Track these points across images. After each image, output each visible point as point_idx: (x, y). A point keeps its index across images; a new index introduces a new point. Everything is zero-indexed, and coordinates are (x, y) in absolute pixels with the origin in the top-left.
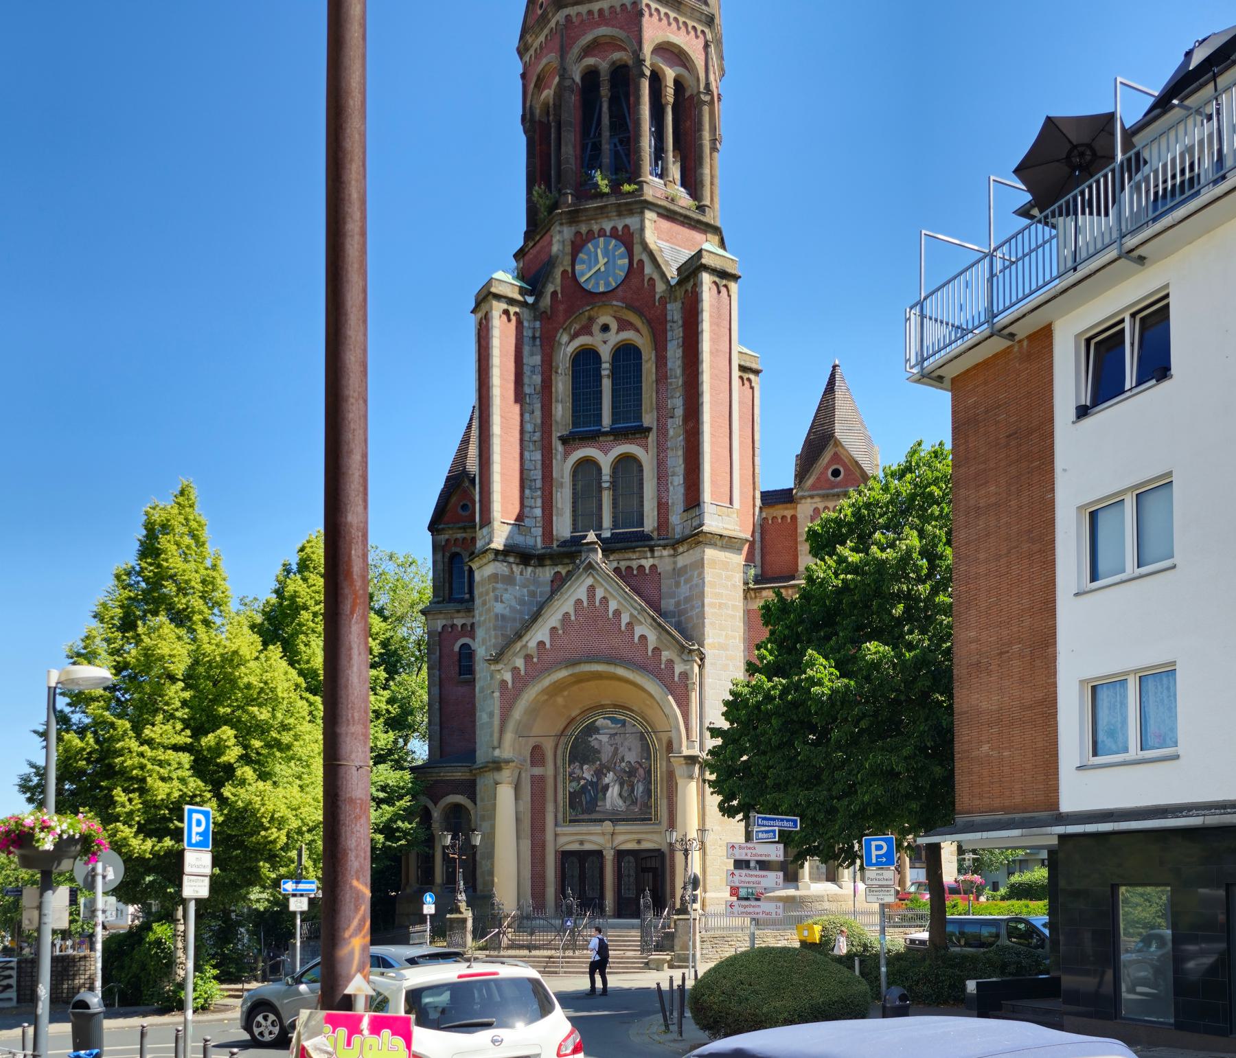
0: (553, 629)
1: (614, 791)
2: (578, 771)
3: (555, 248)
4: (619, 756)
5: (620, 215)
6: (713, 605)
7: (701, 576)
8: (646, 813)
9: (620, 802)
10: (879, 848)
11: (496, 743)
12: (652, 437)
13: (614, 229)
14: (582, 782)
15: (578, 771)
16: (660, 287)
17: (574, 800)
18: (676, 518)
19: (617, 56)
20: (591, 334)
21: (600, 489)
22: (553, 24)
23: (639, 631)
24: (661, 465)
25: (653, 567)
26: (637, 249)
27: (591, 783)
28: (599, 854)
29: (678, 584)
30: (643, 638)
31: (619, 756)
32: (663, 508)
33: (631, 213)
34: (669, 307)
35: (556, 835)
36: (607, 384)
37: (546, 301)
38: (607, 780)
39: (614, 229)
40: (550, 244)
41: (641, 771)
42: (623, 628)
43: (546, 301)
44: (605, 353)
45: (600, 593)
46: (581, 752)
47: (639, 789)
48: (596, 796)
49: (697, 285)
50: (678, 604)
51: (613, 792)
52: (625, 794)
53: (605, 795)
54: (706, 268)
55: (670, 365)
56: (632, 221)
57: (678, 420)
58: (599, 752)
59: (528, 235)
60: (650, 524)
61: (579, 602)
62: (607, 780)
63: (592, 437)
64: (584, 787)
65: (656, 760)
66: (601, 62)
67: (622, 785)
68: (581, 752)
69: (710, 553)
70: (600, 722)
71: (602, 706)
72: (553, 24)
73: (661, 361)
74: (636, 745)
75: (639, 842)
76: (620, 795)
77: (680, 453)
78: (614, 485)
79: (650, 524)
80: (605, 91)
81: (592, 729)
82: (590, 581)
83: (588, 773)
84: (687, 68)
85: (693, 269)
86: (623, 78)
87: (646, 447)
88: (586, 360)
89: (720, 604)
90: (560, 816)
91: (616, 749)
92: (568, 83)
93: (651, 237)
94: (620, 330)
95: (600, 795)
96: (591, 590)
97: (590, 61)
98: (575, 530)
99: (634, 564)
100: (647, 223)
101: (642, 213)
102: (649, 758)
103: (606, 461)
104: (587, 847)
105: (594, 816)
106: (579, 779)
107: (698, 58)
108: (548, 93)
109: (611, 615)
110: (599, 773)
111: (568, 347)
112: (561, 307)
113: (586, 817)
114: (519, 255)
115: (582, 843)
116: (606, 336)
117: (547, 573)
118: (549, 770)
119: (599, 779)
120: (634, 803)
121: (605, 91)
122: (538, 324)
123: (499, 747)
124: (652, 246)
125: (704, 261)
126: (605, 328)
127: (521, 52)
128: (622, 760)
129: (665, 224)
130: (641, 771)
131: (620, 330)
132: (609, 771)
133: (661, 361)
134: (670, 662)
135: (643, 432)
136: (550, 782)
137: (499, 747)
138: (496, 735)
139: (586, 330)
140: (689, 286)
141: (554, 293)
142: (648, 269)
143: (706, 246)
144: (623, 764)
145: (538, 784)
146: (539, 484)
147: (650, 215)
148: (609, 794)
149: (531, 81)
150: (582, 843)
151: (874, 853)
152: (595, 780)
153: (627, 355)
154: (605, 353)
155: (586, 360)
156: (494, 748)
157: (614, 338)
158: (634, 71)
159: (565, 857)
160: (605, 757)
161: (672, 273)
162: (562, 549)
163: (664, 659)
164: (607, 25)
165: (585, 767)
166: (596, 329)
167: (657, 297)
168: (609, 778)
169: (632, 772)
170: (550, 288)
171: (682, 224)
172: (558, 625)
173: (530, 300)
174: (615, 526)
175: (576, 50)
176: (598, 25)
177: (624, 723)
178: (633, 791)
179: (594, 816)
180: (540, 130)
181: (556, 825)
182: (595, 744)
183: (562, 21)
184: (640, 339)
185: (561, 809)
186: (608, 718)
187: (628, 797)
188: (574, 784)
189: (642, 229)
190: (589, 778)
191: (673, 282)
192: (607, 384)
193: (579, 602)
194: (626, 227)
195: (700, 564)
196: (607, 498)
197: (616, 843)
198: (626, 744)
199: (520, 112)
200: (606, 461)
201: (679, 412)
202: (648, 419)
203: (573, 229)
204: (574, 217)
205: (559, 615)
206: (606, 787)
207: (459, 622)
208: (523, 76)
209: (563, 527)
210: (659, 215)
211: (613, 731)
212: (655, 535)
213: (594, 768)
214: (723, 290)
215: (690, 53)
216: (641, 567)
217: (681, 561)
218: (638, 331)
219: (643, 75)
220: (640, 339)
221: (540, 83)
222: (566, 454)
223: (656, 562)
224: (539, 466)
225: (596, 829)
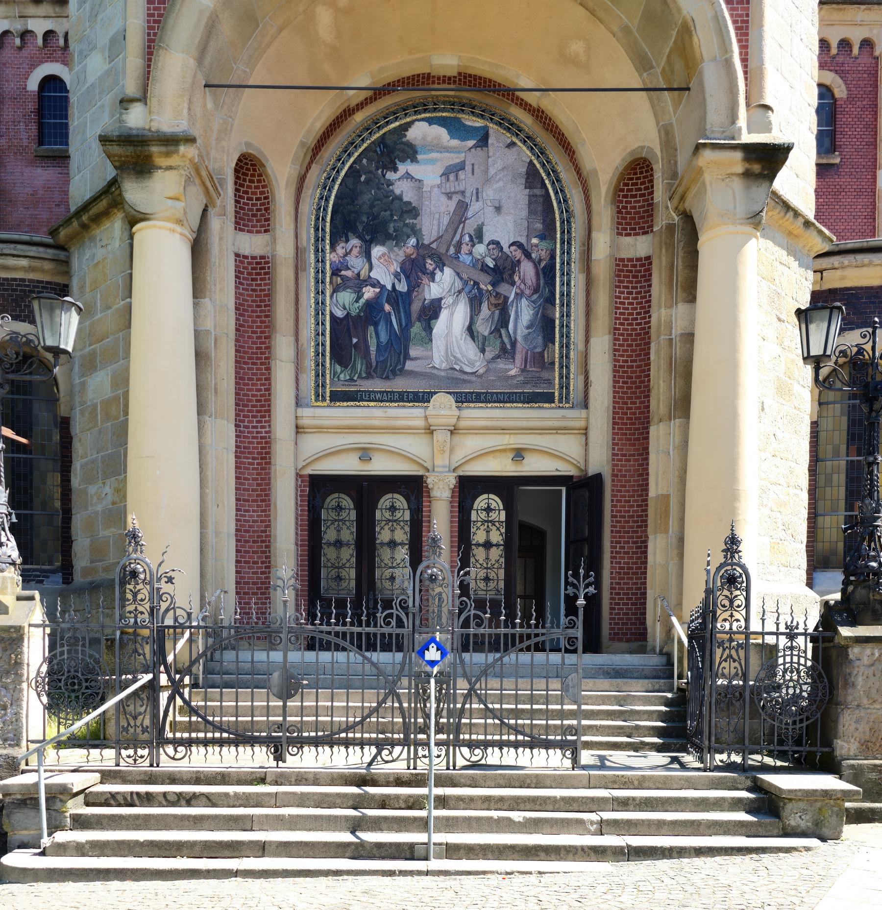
1: (453, 320)
2: (357, 263)
4: (470, 227)
8: (539, 381)
11: (131, 88)
14: (369, 293)
15: (357, 263)
17: (344, 340)
27: (394, 297)
28: (413, 487)
31: (470, 227)
35: (299, 429)
38: (433, 290)
41: (527, 270)
46: (362, 211)
47: (523, 315)
48: (406, 328)
51: (453, 320)
52: (483, 329)
53: (429, 329)
58: (413, 211)
62: (433, 290)
64: (372, 307)
65: (567, 242)
67: (475, 304)
68: (362, 211)
70: (420, 131)
74: (516, 197)
75: (519, 454)
76: (471, 331)
81: (394, 151)
83: (383, 267)
90: (309, 381)
91: (463, 207)
95: (416, 329)
104: (381, 466)
105: (399, 384)
106: (359, 283)
110: (415, 270)
113: (377, 385)
115: (365, 454)
118: (284, 250)
119: (414, 286)
120: (507, 352)
123: (143, 98)
128: (478, 236)
130: (527, 270)
132: (441, 264)
136: (284, 275)
137: (143, 98)
138: (133, 60)
144: (480, 249)
145: (255, 274)
148: (439, 326)
150: (365, 454)
152: (402, 287)
156: (125, 102)
159: (318, 488)
160: (432, 224)
165: (377, 251)
168: (442, 284)
169: (502, 271)
178: (504, 321)
179: (399, 384)
181: (298, 404)
182: (403, 189)
185: (310, 364)
186: (443, 122)
187: (495, 338)
188: (346, 296)
190: (387, 281)
197: (459, 455)
198: (489, 193)
206: (432, 310)
211: (455, 159)
213: (400, 254)
225: (411, 415)
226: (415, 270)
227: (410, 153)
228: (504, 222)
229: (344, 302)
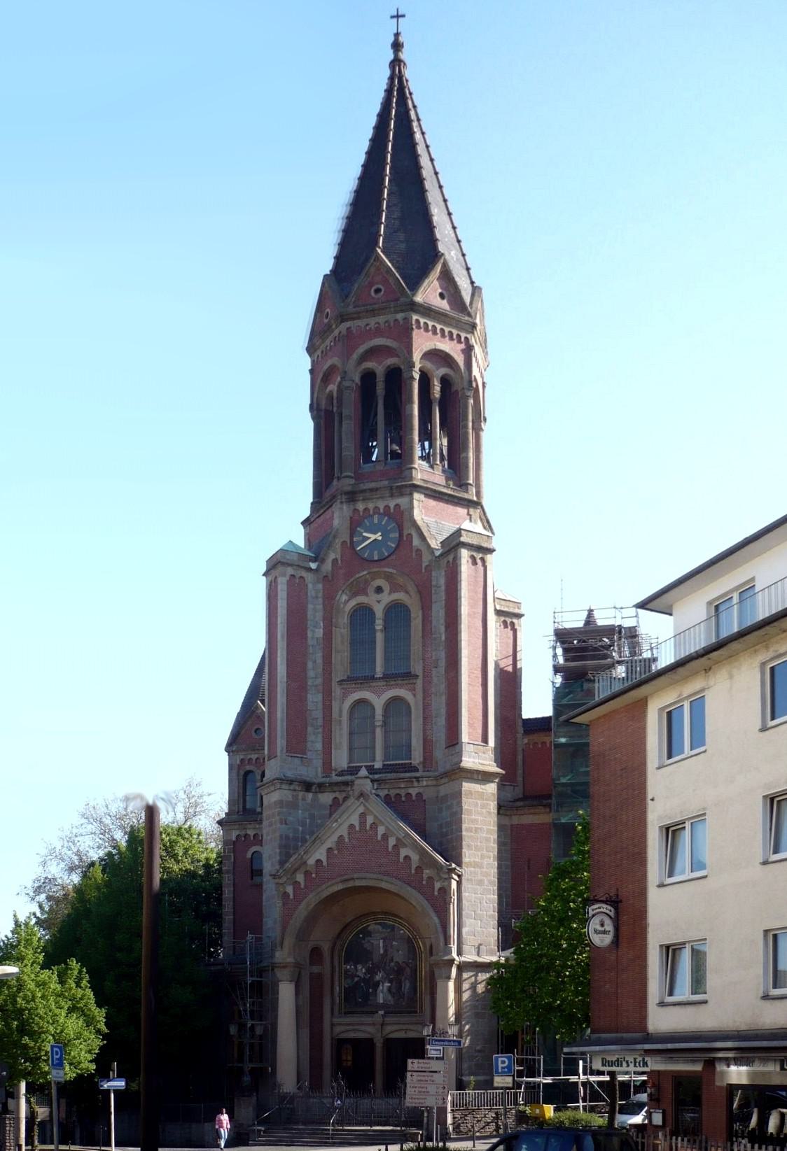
0: (330, 849)
3: (336, 522)
5: (392, 496)
6: (469, 830)
7: (460, 803)
9: (390, 998)
10: (503, 1062)
12: (419, 682)
13: (387, 507)
16: (426, 559)
17: (349, 994)
18: (439, 753)
19: (391, 361)
20: (367, 594)
21: (374, 727)
22: (336, 333)
23: (404, 852)
24: (426, 707)
25: (419, 795)
26: (406, 524)
27: (364, 980)
28: (369, 1042)
29: (440, 810)
30: (407, 857)
32: (427, 744)
33: (402, 495)
34: (434, 574)
35: (332, 1025)
36: (380, 637)
37: (328, 566)
38: (378, 978)
39: (387, 507)
40: (332, 518)
41: (408, 970)
42: (390, 849)
43: (328, 566)
44: (379, 611)
45: (370, 820)
47: (406, 986)
49: (456, 560)
50: (441, 826)
54: (465, 545)
55: (434, 623)
56: (402, 501)
57: (442, 670)
59: (315, 506)
60: (417, 758)
61: (352, 827)
63: (367, 680)
66: (379, 367)
67: (390, 981)
68: (356, 952)
69: (467, 786)
70: (373, 927)
71: (374, 913)
72: (336, 333)
73: (426, 619)
77: (444, 698)
78: (385, 723)
79: (417, 758)
80: (380, 389)
82: (361, 809)
83: (361, 970)
84: (451, 368)
85: (454, 543)
86: (396, 378)
87: (413, 690)
88: (362, 616)
89: (476, 829)
90: (336, 1009)
92: (347, 384)
93: (418, 515)
94: (391, 591)
96: (363, 817)
97: (370, 365)
98: (350, 761)
99: (403, 793)
100: (415, 503)
101: (411, 494)
102: (414, 959)
103: (378, 702)
106: (353, 976)
107: (460, 359)
108: (332, 388)
109: (379, 837)
110: (371, 971)
111: (347, 603)
112: (342, 571)
114: (306, 523)
116: (379, 597)
117: (326, 798)
121: (380, 389)
122: (320, 586)
124: (420, 523)
125: (462, 539)
126: (379, 590)
127: (311, 349)
128: (392, 960)
129: (432, 503)
130: (408, 970)
131: (391, 591)
133: (426, 619)
134: (430, 879)
135: (409, 676)
139: (364, 592)
140: (451, 558)
141: (335, 561)
142: (416, 542)
143: (467, 525)
145: (316, 980)
146: (320, 722)
147: (416, 496)
149: (320, 377)
151: (500, 1065)
153: (397, 613)
154: (379, 611)
155: (362, 616)
157: (386, 598)
158: (405, 375)
159: (340, 1044)
160: (376, 958)
161: (435, 544)
162: (340, 779)
163: (425, 876)
164: (382, 336)
166: (371, 590)
167: (424, 565)
169: (399, 971)
170: (332, 556)
171: (447, 502)
172: (333, 846)
173: (313, 566)
174: (386, 757)
175: (355, 356)
176: (375, 337)
177: (393, 928)
180: (325, 415)
183: (344, 332)
184: (409, 599)
188: (349, 981)
189: (412, 508)
191: (437, 553)
192: (380, 637)
193: (352, 827)
194: (397, 505)
195: (458, 795)
196: (379, 732)
199: (308, 402)
200: (378, 702)
201: (442, 663)
202: (417, 668)
203: (352, 507)
204: (352, 497)
205: (334, 838)
206: (377, 984)
207: (251, 833)
208: (312, 371)
209: (341, 759)
210: (427, 496)
212: (420, 767)
214: (479, 561)
215: (452, 354)
216: (408, 794)
217: (443, 790)
218: (407, 592)
219: (412, 378)
220: (409, 599)
221: (326, 378)
222: (344, 696)
223: (421, 790)
224: (320, 706)
226: (371, 971)
227: (369, 934)
228: (400, 956)
229: (347, 983)
